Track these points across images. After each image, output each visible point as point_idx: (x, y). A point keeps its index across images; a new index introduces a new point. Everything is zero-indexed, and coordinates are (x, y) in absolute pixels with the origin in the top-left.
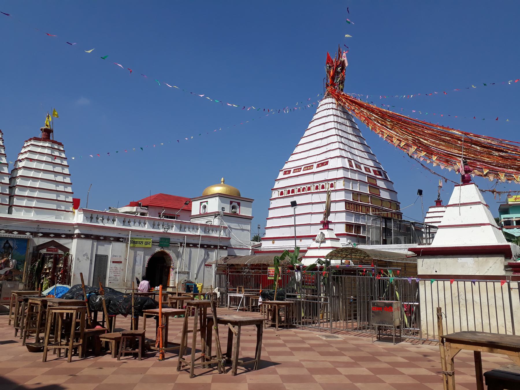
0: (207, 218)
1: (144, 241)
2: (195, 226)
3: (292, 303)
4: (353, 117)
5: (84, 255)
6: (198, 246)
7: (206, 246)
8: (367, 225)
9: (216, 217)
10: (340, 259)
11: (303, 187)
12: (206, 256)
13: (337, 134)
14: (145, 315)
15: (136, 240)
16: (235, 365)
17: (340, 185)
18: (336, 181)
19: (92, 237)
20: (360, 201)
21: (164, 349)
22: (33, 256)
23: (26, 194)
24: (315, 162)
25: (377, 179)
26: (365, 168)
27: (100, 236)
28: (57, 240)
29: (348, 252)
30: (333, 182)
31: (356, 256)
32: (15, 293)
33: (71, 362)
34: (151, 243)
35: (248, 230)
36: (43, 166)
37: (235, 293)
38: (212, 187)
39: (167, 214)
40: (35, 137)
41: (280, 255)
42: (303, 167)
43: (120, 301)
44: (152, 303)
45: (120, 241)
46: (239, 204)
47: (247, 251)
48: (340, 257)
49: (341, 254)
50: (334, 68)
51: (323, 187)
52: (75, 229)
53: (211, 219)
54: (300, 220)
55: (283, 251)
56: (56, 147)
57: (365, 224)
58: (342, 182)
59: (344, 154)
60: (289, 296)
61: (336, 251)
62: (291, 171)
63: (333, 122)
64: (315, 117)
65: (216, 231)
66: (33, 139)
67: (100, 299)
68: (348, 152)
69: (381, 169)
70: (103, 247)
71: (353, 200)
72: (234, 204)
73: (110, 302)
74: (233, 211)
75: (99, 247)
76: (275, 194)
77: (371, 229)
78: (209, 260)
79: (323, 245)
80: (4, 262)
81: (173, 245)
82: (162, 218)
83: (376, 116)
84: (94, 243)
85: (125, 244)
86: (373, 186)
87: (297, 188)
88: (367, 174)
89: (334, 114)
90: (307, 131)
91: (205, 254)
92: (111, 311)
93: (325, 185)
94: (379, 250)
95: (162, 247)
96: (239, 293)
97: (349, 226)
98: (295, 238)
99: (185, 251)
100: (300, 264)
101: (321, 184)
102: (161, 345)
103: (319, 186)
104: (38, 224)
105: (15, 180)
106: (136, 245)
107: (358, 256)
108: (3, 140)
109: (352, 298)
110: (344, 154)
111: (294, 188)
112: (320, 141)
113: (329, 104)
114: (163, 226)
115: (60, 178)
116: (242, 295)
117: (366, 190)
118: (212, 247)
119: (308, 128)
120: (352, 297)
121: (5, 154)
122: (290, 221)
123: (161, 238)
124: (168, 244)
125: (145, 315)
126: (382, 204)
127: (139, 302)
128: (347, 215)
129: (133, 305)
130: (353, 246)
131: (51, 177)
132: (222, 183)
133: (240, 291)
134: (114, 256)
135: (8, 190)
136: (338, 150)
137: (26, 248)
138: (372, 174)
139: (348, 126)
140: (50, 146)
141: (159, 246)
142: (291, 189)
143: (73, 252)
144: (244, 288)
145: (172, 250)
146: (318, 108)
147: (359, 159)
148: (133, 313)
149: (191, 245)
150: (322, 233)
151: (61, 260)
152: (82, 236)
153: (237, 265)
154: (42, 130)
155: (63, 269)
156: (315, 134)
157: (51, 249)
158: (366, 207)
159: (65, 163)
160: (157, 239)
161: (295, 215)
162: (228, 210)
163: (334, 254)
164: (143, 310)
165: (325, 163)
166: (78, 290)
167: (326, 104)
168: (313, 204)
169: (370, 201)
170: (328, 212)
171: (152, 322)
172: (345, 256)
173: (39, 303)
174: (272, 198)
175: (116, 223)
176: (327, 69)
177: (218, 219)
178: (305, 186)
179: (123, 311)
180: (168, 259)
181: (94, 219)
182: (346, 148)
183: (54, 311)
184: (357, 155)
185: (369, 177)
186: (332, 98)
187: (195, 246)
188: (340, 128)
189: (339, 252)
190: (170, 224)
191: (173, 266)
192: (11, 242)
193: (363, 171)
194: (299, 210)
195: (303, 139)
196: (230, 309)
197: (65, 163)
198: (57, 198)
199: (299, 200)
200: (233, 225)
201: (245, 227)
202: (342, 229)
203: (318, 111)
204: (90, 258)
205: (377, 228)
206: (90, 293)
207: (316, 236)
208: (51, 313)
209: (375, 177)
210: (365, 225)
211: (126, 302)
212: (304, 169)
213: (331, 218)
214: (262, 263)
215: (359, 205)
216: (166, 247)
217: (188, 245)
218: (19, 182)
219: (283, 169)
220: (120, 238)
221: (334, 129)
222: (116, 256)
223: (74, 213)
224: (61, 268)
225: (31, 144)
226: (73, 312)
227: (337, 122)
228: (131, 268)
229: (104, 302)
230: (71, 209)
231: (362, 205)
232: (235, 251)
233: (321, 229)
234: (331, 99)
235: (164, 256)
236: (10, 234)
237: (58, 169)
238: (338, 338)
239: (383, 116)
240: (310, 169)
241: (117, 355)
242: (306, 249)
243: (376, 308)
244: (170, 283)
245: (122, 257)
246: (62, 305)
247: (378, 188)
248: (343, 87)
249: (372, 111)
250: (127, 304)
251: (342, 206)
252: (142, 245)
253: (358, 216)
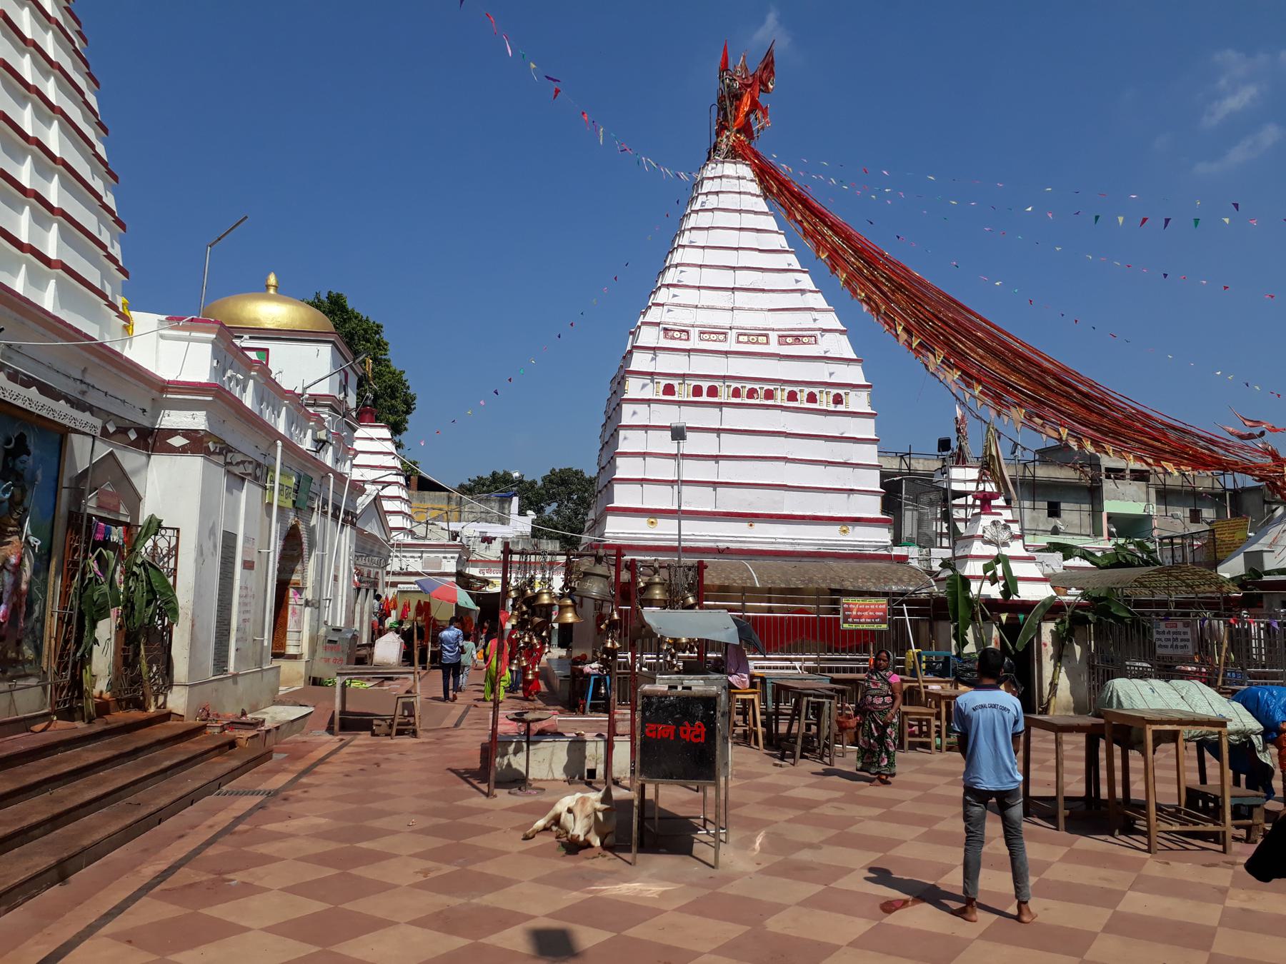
11: (749, 386)
24: (773, 330)
30: (841, 392)
52: (159, 406)
54: (692, 470)
93: (818, 395)
111: (716, 384)
112: (759, 274)
132: (272, 291)
178: (757, 387)
244: (288, 642)
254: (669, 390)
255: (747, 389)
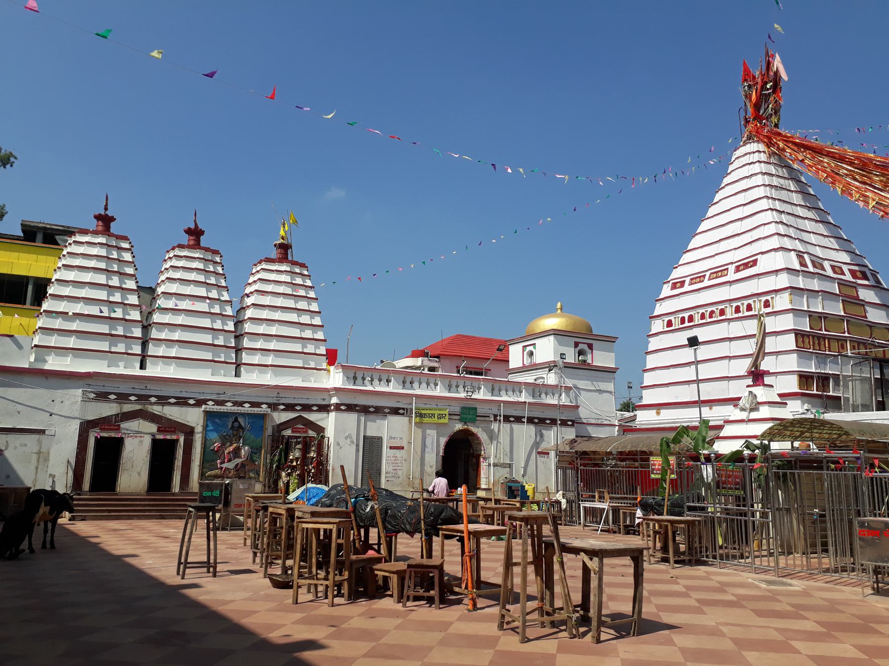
0: (536, 373)
1: (437, 412)
2: (517, 387)
3: (699, 521)
4: (801, 173)
5: (346, 438)
6: (523, 420)
7: (536, 421)
8: (843, 375)
9: (552, 370)
10: (789, 439)
11: (709, 309)
12: (538, 437)
13: (772, 207)
14: (442, 534)
15: (423, 412)
16: (596, 625)
17: (782, 302)
18: (774, 296)
19: (357, 408)
20: (826, 331)
21: (475, 593)
22: (273, 441)
23: (259, 344)
24: (732, 263)
25: (858, 287)
26: (833, 267)
27: (369, 407)
28: (306, 415)
29: (804, 428)
30: (769, 298)
31: (821, 433)
32: (250, 497)
33: (333, 606)
34: (447, 415)
35: (610, 392)
36: (280, 302)
37: (592, 501)
38: (542, 318)
39: (469, 368)
40: (266, 258)
41: (671, 435)
42: (708, 274)
43: (402, 511)
44: (453, 516)
45: (400, 414)
46: (590, 347)
47: (611, 428)
48: (789, 436)
49: (791, 431)
50: (759, 86)
51: (749, 308)
52: (331, 397)
53: (543, 373)
54: (706, 371)
55: (677, 428)
56: (298, 271)
57: (839, 373)
58: (786, 295)
59: (787, 243)
60: (691, 509)
61: (779, 425)
62: (684, 281)
63: (762, 187)
64: (727, 180)
65: (553, 395)
66: (265, 261)
67: (372, 508)
68: (795, 239)
69: (866, 266)
70: (374, 423)
71: (811, 328)
72: (581, 346)
73: (386, 513)
74: (580, 358)
75: (369, 423)
76: (658, 326)
77: (850, 383)
78: (543, 443)
79: (754, 415)
80: (234, 450)
81: (482, 418)
82: (462, 375)
83: (849, 168)
84: (361, 418)
85: (406, 419)
86: (851, 301)
87: (698, 313)
88: (837, 279)
89: (764, 172)
90: (712, 207)
91: (536, 435)
92: (389, 527)
93: (753, 304)
94: (870, 421)
95: (465, 423)
96: (600, 502)
97: (805, 379)
98: (699, 403)
99: (504, 429)
100: (712, 449)
101: (746, 303)
102: (470, 585)
103: (741, 306)
104: (278, 391)
105: (243, 324)
106: (424, 419)
107: (826, 433)
108: (223, 266)
109: (817, 513)
110: (787, 243)
111: (692, 313)
112: (739, 223)
113: (752, 155)
114: (464, 387)
115: (305, 319)
116: (604, 506)
117: (837, 309)
118: (548, 422)
119: (714, 202)
120: (817, 510)
121: (226, 287)
122: (689, 374)
123: (463, 408)
124: (474, 416)
125: (442, 534)
126: (871, 334)
127: (432, 513)
128: (799, 357)
129: (422, 518)
130: (815, 415)
131: (293, 317)
132: (559, 311)
133: (601, 498)
134: (391, 438)
135: (233, 340)
136: (776, 237)
137: (262, 428)
138: (848, 277)
139: (792, 191)
140: (288, 269)
141: (460, 420)
142: (686, 315)
143: (330, 433)
144: (609, 493)
145: (481, 427)
146: (732, 163)
147: (819, 252)
148: (423, 531)
149: (512, 419)
150: (750, 392)
151: (313, 446)
152: (343, 407)
153: (594, 453)
154: (275, 245)
155: (317, 460)
156: (729, 210)
157: (295, 428)
158: (838, 340)
159: (312, 294)
160: (457, 410)
161: (697, 363)
162: (571, 357)
163: (777, 431)
164: (438, 527)
165: (751, 264)
166: (339, 493)
167: (745, 154)
168: (730, 339)
169: (846, 330)
170: (760, 353)
171: (453, 546)
172: (798, 434)
173: (283, 512)
174: (651, 333)
175: (391, 384)
176: (745, 91)
177: (555, 373)
178: (714, 309)
179: (408, 527)
180: (476, 442)
181: (359, 380)
182: (791, 232)
183: (305, 526)
184: (815, 243)
185: (842, 284)
186: (758, 142)
187: (518, 420)
188: (777, 196)
189: (785, 428)
190: (475, 384)
191: (485, 453)
192: (241, 420)
193: (829, 272)
194: (704, 352)
195: (705, 221)
196: (586, 528)
197: (312, 294)
198: (303, 349)
199: (702, 334)
200: (581, 384)
201: (603, 386)
202: (792, 384)
203: (731, 168)
204: (355, 441)
205: (863, 380)
206: (356, 498)
207: (739, 399)
208: (300, 528)
209: (856, 283)
210: (839, 375)
211: (412, 512)
212: (710, 276)
213: (764, 366)
214: (638, 449)
215: (824, 337)
216: (471, 422)
217: (507, 419)
218: (248, 327)
219: (669, 280)
220: (400, 409)
221: (765, 200)
222: (394, 438)
223: (329, 371)
224: (313, 458)
225: (262, 269)
226: (332, 528)
227: (769, 185)
228: (418, 458)
229: (378, 512)
230: (324, 365)
231: (830, 338)
232: (590, 428)
233: (748, 386)
234: (756, 144)
235: (470, 438)
236: (240, 408)
237: (302, 305)
238: (791, 585)
239: (864, 166)
240: (721, 276)
241: (401, 598)
242: (721, 423)
243: (866, 533)
244: (482, 483)
245: (404, 439)
246: (316, 517)
247: (863, 304)
248: (778, 121)
249: (842, 159)
250: (413, 516)
251: (789, 342)
252: (434, 419)
253: (822, 359)
254: (670, 324)
255: (709, 312)
